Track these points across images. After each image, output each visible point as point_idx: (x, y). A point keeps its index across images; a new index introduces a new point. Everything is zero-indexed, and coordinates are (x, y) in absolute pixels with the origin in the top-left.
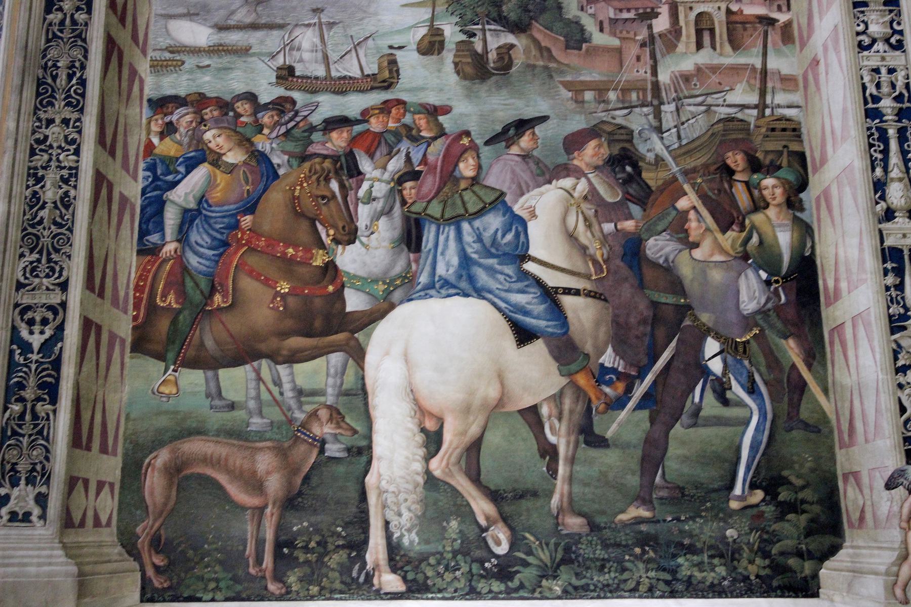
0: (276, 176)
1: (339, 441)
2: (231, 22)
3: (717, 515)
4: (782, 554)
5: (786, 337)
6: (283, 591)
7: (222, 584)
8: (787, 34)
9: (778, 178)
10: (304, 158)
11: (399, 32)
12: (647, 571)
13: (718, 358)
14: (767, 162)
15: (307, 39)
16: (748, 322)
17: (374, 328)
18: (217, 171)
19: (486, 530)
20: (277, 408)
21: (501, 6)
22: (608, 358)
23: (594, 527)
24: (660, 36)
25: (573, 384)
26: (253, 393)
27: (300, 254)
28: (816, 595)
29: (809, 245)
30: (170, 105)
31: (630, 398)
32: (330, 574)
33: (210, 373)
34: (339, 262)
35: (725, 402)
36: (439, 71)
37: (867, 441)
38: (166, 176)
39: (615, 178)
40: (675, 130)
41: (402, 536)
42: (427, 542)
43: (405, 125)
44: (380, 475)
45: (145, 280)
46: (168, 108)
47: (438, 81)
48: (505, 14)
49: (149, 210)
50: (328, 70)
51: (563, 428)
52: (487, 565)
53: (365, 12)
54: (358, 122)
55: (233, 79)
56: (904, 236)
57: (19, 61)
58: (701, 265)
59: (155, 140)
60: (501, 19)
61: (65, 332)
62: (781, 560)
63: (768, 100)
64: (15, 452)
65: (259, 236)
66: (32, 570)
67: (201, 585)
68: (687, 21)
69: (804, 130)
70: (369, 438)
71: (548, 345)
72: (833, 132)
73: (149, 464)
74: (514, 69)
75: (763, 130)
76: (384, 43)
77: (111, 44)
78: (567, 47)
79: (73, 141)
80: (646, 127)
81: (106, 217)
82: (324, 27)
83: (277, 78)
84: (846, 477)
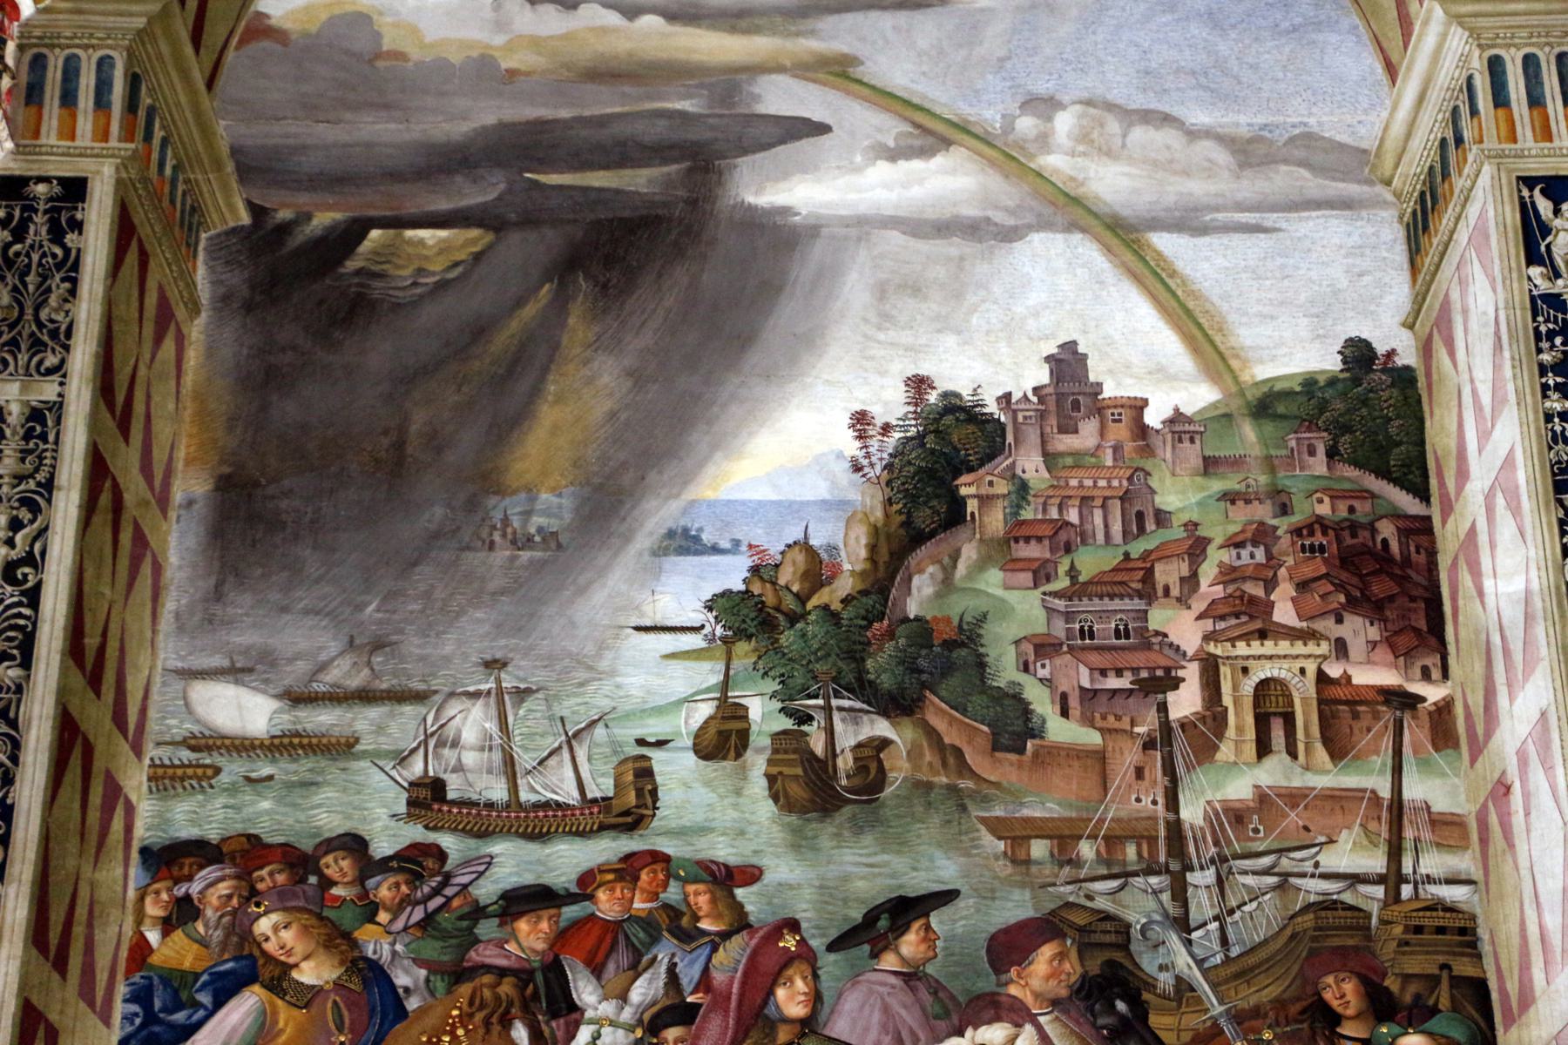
0: (402, 1015)
2: (320, 687)
10: (458, 973)
11: (659, 711)
14: (1408, 998)
18: (280, 1002)
21: (863, 660)
24: (1183, 726)
30: (187, 861)
36: (738, 792)
38: (172, 1012)
39: (1094, 1025)
40: (1214, 926)
43: (666, 907)
46: (181, 868)
47: (735, 815)
48: (872, 677)
50: (514, 788)
53: (590, 668)
54: (570, 898)
55: (319, 806)
59: (153, 937)
60: (862, 687)
63: (1407, 866)
68: (1237, 695)
69: (1483, 933)
74: (888, 791)
75: (1398, 930)
76: (628, 733)
77: (68, 731)
78: (996, 747)
80: (1157, 917)
82: (507, 697)
83: (410, 803)
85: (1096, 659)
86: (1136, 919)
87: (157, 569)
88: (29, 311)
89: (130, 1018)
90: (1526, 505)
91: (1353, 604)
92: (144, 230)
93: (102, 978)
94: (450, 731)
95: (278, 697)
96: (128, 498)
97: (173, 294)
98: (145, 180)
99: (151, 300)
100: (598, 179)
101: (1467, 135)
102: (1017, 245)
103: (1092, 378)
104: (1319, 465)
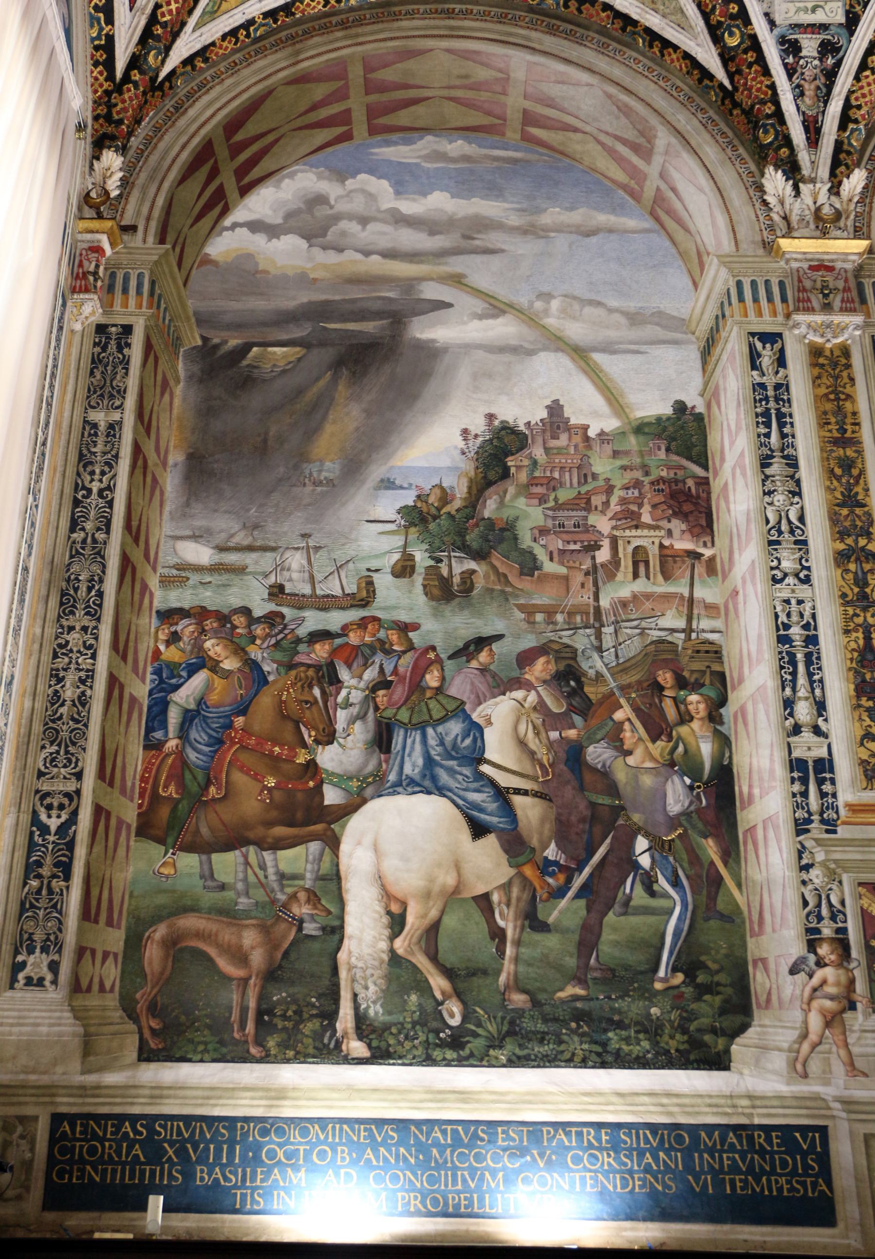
0: (266, 682)
1: (315, 921)
2: (230, 544)
3: (643, 994)
4: (699, 1030)
5: (706, 837)
6: (263, 1054)
7: (210, 1047)
8: (711, 567)
9: (701, 695)
10: (290, 666)
11: (376, 556)
12: (581, 1043)
13: (647, 854)
14: (692, 680)
15: (296, 560)
16: (674, 822)
17: (348, 821)
19: (442, 1003)
20: (262, 890)
22: (551, 852)
23: (536, 1003)
25: (520, 875)
26: (241, 875)
27: (286, 752)
28: (726, 1068)
29: (727, 755)
31: (569, 888)
32: (305, 1040)
33: (204, 857)
34: (319, 760)
35: (652, 894)
36: (410, 592)
37: (774, 931)
38: (170, 679)
41: (368, 1007)
42: (390, 1013)
43: (379, 640)
44: (350, 952)
45: (150, 773)
49: (155, 709)
51: (511, 913)
52: (442, 1035)
54: (338, 636)
56: (809, 749)
57: (46, 575)
58: (634, 770)
59: (162, 648)
60: (464, 547)
61: (79, 817)
62: (697, 1035)
63: (694, 626)
64: (32, 923)
65: (251, 735)
66: (44, 1029)
67: (191, 1047)
68: (625, 554)
69: (724, 653)
70: (341, 918)
71: (499, 838)
72: (749, 655)
73: (149, 937)
74: (475, 592)
75: (690, 652)
76: (363, 566)
77: (126, 562)
78: (522, 574)
79: (90, 647)
81: (117, 715)
83: (270, 594)
84: (755, 962)
85: (566, 537)
86: (580, 647)
87: (162, 493)
88: (108, 382)
89: (153, 681)
90: (749, 472)
91: (675, 514)
92: (156, 347)
93: (141, 664)
94: (286, 564)
95: (213, 548)
96: (150, 463)
97: (169, 376)
98: (157, 326)
99: (159, 377)
100: (351, 326)
101: (727, 313)
102: (534, 357)
103: (566, 415)
104: (662, 454)
